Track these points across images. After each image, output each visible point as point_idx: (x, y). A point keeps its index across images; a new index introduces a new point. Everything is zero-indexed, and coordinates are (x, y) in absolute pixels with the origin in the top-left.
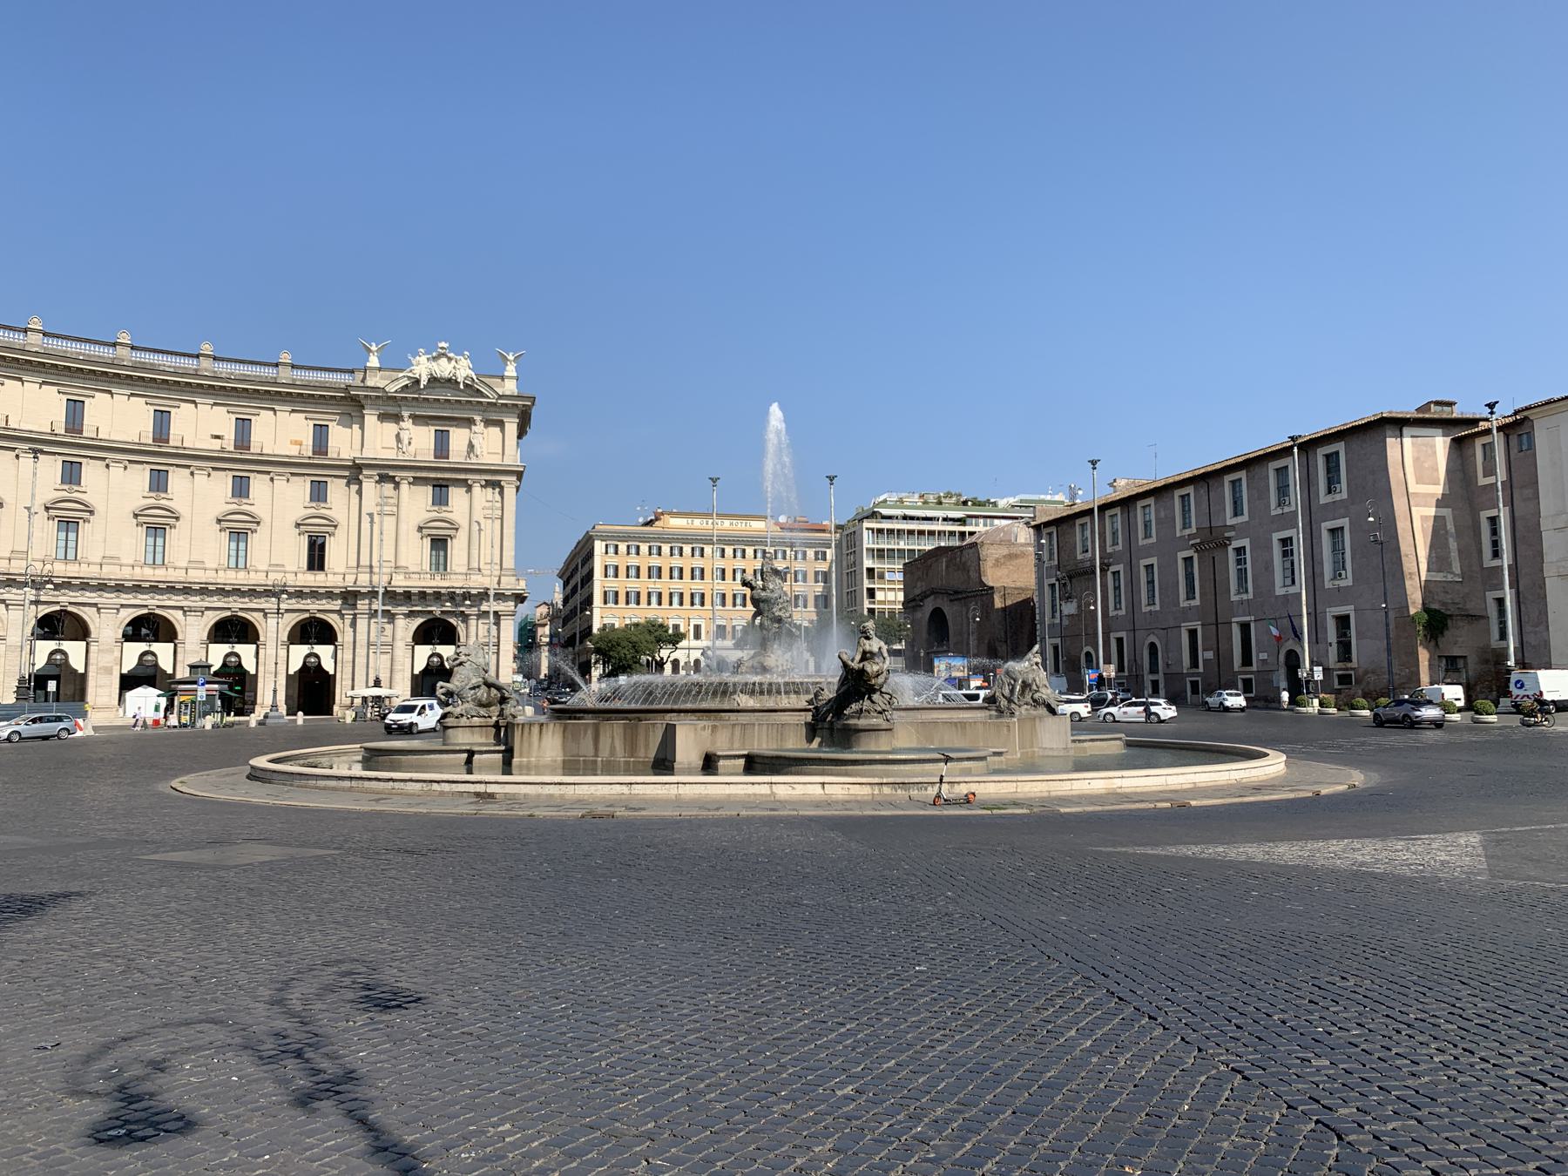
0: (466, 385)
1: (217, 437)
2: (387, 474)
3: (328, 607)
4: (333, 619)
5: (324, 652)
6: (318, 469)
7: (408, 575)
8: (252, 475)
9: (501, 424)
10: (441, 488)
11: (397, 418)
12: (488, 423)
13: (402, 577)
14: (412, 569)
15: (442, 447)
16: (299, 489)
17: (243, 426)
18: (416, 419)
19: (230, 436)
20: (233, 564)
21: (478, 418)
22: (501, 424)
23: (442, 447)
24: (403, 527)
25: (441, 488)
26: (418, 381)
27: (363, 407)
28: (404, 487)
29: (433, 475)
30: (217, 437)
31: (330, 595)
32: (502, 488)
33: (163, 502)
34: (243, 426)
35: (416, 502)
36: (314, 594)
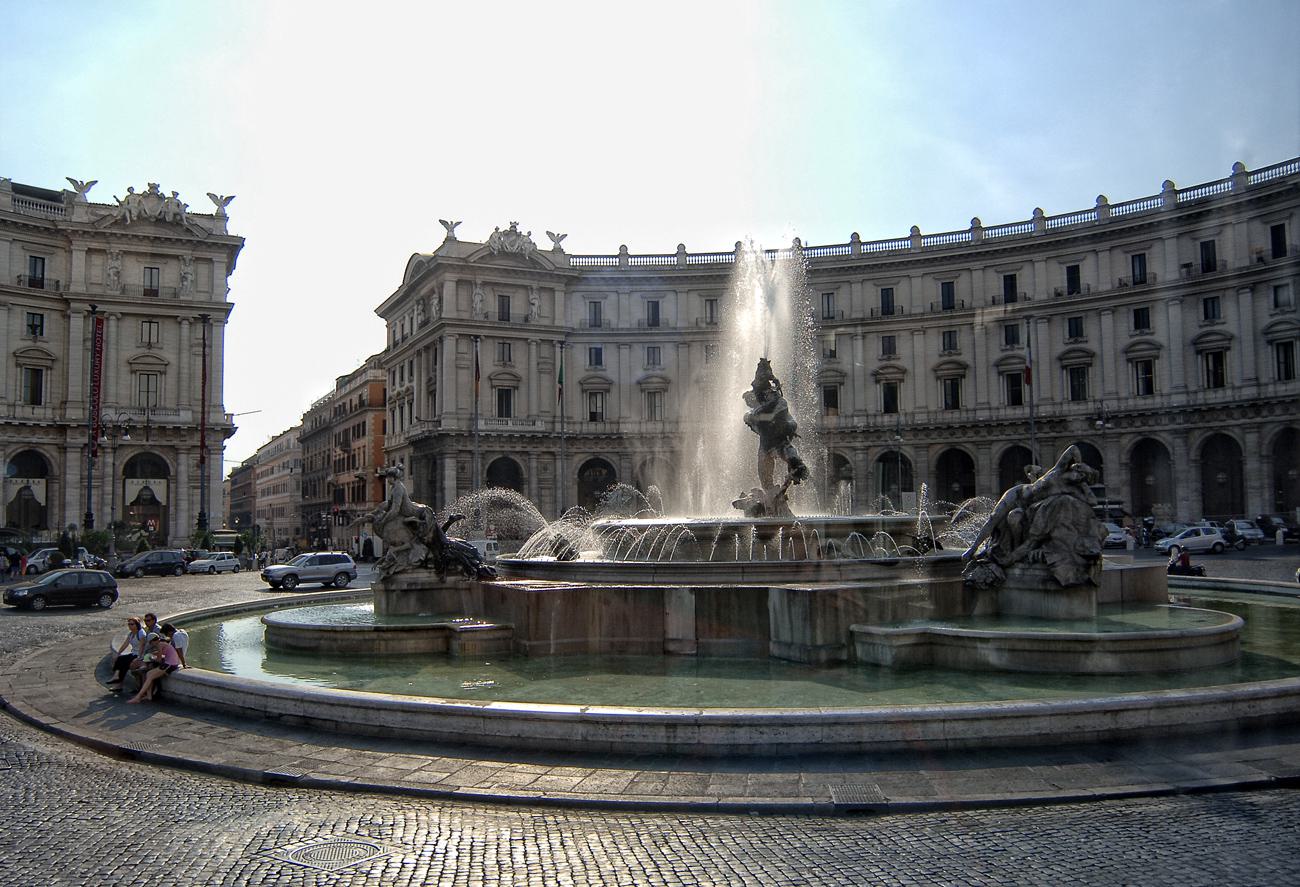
8: (1220, 294)
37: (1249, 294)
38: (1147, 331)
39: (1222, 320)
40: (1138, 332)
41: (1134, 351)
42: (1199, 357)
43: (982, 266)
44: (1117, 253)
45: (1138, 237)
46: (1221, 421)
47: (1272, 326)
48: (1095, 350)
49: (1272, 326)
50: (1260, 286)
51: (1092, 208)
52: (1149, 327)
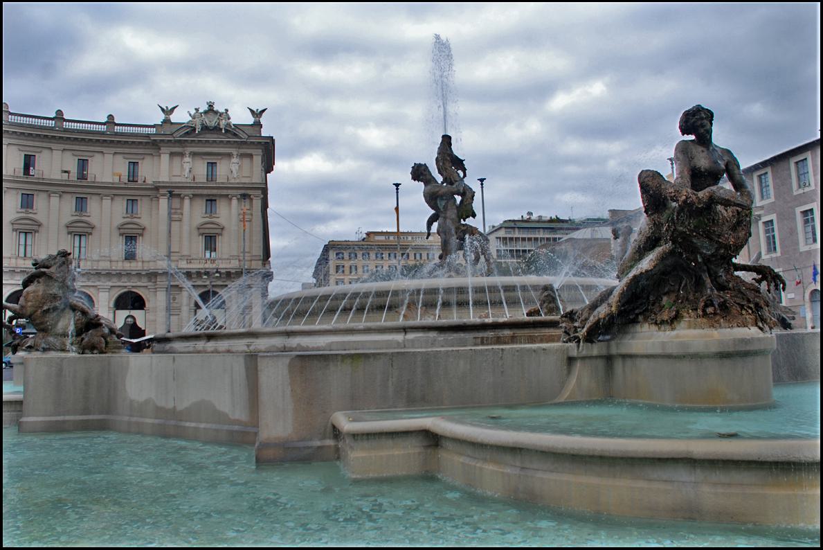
0: (227, 131)
1: (66, 172)
2: (173, 192)
3: (139, 284)
4: (141, 292)
5: (137, 314)
6: (133, 191)
7: (189, 261)
8: (88, 196)
9: (251, 156)
10: (211, 200)
11: (182, 155)
12: (242, 156)
13: (185, 262)
14: (194, 257)
15: (211, 176)
16: (120, 206)
17: (83, 164)
18: (194, 154)
19: (74, 169)
20: (22, 254)
21: (235, 153)
22: (251, 156)
23: (211, 176)
24: (186, 228)
25: (211, 200)
26: (194, 129)
27: (160, 149)
28: (187, 202)
29: (205, 192)
30: (66, 172)
31: (139, 275)
32: (252, 199)
33: (31, 216)
34: (83, 164)
35: (194, 213)
36: (129, 274)
37: (110, 201)
38: (30, 211)
39: (88, 214)
40: (24, 210)
41: (71, 227)
42: (70, 236)
43: (113, 152)
44: (68, 154)
45: (78, 147)
46: (82, 282)
47: (125, 224)
48: (96, 224)
49: (125, 224)
50: (116, 198)
51: (52, 117)
52: (32, 208)
